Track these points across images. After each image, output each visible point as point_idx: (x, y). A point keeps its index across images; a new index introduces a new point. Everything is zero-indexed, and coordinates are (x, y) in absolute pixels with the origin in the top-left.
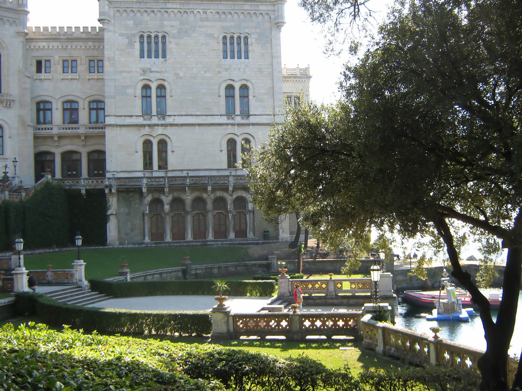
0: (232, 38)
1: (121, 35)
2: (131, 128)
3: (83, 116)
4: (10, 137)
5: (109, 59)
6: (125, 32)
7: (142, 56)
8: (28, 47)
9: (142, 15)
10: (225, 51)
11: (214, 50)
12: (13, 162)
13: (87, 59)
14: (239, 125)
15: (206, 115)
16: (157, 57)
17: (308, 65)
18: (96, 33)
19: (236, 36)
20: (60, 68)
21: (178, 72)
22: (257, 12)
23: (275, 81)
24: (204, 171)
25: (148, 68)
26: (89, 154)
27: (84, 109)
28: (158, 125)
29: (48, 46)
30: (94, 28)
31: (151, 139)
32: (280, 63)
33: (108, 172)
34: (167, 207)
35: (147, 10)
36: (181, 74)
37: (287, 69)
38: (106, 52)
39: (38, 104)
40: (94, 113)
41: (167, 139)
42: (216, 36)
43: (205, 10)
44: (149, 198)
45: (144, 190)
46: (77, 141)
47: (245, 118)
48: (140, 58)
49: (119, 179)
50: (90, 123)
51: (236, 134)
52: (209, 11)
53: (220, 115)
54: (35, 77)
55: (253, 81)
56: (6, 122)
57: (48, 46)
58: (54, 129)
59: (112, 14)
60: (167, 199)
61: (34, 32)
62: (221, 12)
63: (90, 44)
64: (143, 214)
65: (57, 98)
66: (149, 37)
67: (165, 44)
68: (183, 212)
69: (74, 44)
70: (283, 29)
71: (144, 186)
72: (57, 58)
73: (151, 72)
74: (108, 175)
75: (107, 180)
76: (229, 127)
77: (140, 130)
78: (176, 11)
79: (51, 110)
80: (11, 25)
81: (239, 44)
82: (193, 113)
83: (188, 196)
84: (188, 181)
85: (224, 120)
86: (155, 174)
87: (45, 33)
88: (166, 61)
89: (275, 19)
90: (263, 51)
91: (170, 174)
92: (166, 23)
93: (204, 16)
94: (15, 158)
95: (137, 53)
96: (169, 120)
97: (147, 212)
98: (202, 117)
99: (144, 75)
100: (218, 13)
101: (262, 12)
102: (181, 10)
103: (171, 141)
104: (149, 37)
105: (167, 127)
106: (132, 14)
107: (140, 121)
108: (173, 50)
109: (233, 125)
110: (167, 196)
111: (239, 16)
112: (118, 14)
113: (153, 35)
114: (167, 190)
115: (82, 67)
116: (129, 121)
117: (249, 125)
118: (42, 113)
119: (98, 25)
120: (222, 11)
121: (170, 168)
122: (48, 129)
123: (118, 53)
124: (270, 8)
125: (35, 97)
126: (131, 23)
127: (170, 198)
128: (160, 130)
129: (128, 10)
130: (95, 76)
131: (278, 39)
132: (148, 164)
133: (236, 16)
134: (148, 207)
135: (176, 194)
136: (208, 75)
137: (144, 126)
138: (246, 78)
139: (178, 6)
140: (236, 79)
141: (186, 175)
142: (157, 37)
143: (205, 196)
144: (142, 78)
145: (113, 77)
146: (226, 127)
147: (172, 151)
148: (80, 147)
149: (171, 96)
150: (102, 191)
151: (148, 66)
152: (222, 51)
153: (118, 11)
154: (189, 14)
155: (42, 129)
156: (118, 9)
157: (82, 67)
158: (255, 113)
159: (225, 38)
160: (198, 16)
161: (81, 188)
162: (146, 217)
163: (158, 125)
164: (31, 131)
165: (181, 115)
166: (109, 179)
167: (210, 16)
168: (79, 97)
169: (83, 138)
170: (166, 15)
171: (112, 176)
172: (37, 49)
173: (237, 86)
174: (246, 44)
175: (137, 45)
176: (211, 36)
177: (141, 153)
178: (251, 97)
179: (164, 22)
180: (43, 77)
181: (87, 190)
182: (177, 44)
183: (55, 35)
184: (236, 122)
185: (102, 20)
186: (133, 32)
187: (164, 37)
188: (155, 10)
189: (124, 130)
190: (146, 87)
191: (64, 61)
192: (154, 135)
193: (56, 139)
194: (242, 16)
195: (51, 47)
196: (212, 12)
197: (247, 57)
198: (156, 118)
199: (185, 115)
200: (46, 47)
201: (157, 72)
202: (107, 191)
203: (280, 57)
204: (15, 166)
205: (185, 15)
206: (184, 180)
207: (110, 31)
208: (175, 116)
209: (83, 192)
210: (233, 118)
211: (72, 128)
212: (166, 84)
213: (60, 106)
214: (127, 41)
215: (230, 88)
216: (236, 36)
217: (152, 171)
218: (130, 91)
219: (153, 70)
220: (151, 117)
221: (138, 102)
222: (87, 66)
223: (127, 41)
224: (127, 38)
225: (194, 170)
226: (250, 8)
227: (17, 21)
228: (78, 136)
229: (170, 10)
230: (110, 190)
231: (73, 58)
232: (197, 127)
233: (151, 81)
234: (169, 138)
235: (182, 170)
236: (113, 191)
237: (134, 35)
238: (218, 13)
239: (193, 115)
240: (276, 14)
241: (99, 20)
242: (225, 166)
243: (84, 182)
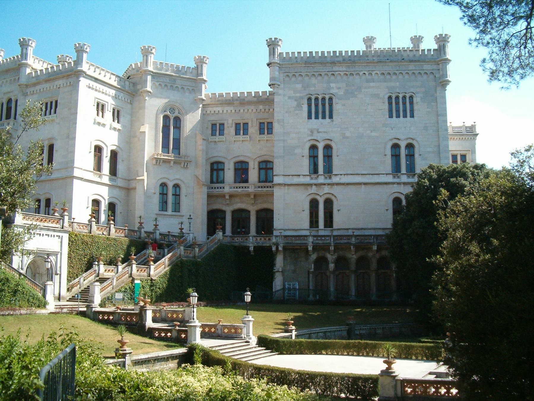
0: (397, 98)
1: (290, 98)
2: (298, 187)
3: (253, 175)
4: (186, 196)
5: (279, 121)
6: (294, 95)
7: (310, 117)
8: (205, 112)
9: (310, 78)
10: (390, 111)
11: (379, 110)
12: (188, 218)
13: (258, 122)
15: (372, 174)
16: (324, 117)
17: (475, 123)
18: (266, 97)
19: (401, 96)
20: (233, 130)
21: (344, 132)
22: (422, 72)
23: (441, 139)
24: (369, 230)
26: (258, 212)
27: (254, 169)
28: (325, 184)
29: (223, 111)
30: (264, 93)
31: (318, 198)
32: (446, 121)
33: (275, 230)
34: (332, 266)
36: (348, 134)
37: (453, 128)
38: (275, 115)
39: (212, 164)
40: (263, 172)
41: (333, 198)
42: (381, 96)
43: (370, 72)
44: (314, 257)
45: (310, 248)
47: (411, 177)
48: (308, 119)
49: (286, 237)
50: (259, 182)
51: (402, 193)
52: (375, 72)
53: (387, 174)
54: (210, 140)
55: (418, 139)
56: (183, 182)
57: (223, 111)
58: (225, 188)
59: (282, 78)
60: (331, 257)
61: (211, 98)
62: (386, 73)
63: (261, 107)
64: (309, 273)
65: (230, 158)
66: (317, 99)
67: (332, 105)
68: (348, 271)
69: (246, 108)
70: (448, 88)
71: (310, 244)
72: (230, 121)
73: (319, 132)
74: (275, 233)
75: (274, 237)
76: (395, 186)
77: (307, 189)
78: (342, 73)
79: (223, 170)
80: (190, 93)
81: (404, 103)
83: (353, 255)
84: (353, 239)
85: (390, 179)
86: (321, 233)
87: (220, 98)
89: (440, 78)
90: (428, 110)
91: (335, 233)
92: (332, 85)
93: (370, 77)
94: (190, 216)
95: (305, 114)
96: (335, 180)
97: (312, 270)
98: (368, 176)
99: (312, 135)
100: (383, 74)
101: (426, 72)
102: (347, 73)
103: (337, 200)
104: (317, 99)
105: (333, 186)
106: (300, 78)
107: (307, 180)
109: (399, 184)
110: (332, 255)
111: (404, 77)
112: (287, 79)
113: (320, 97)
114: (333, 249)
115: (253, 129)
116: (296, 180)
118: (215, 173)
119: (269, 89)
120: (387, 72)
121: (335, 226)
122: (221, 188)
123: (287, 115)
124: (435, 67)
125: (210, 158)
126: (299, 86)
127: (335, 257)
128: (326, 189)
129: (297, 74)
130: (265, 137)
131: (444, 97)
132: (314, 222)
133: (401, 77)
134: (313, 265)
135: (341, 253)
136: (374, 134)
137: (311, 185)
138: (411, 137)
139: (344, 69)
141: (352, 234)
142: (324, 99)
143: (370, 254)
145: (282, 138)
147: (339, 210)
149: (337, 156)
150: (270, 247)
151: (315, 127)
152: (387, 110)
153: (288, 76)
154: (355, 76)
155: (215, 188)
157: (253, 129)
159: (390, 98)
160: (364, 77)
161: (250, 245)
162: (311, 275)
163: (325, 184)
164: (205, 190)
165: (347, 174)
166: (276, 236)
167: (376, 77)
169: (252, 197)
170: (332, 78)
171: (279, 234)
172: (212, 114)
173: (403, 145)
174: (411, 103)
175: (305, 107)
176: (376, 96)
177: (307, 213)
178: (416, 156)
179: (331, 84)
180: (217, 140)
181: (255, 247)
182: (344, 105)
183: (230, 100)
185: (273, 85)
186: (301, 95)
187: (331, 99)
188: (323, 74)
189: (292, 188)
190: (314, 148)
191: (236, 124)
192: (321, 194)
193: (227, 197)
194: (407, 77)
195: (225, 112)
196: (376, 73)
197: (412, 116)
198: (323, 177)
199: (351, 174)
200: (221, 112)
201: (324, 132)
202: (274, 249)
203: (445, 115)
204: (190, 223)
205: (351, 77)
206: (349, 239)
207: (280, 95)
208: (341, 175)
209: (252, 249)
210: (398, 177)
211: (242, 188)
214: (296, 103)
215: (396, 147)
216: (401, 96)
217: (318, 230)
219: (320, 130)
220: (318, 177)
221: (306, 162)
222: (257, 128)
223: (296, 103)
224: (296, 100)
225: (359, 229)
226: (414, 68)
227: (195, 88)
228: (248, 195)
229: (337, 73)
230: (277, 248)
231: (244, 121)
232: (363, 186)
234: (335, 197)
235: (347, 229)
236: (280, 248)
237: (302, 98)
238: (383, 74)
240: (441, 72)
241: (270, 85)
243: (253, 240)
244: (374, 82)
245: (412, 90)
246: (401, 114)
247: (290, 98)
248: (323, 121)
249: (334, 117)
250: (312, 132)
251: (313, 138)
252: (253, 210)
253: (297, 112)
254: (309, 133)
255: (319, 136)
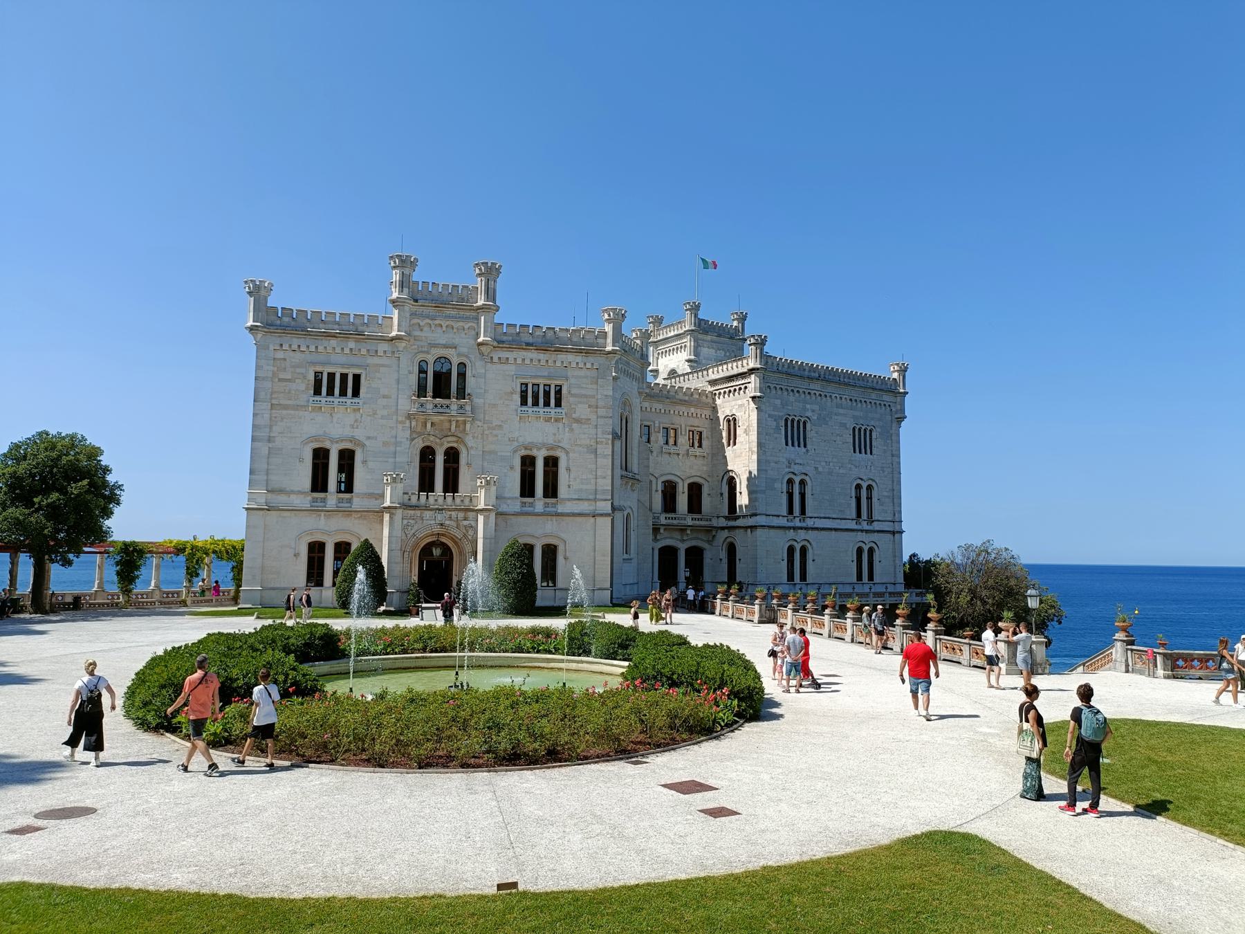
1: (770, 416)
7: (787, 444)
14: (867, 531)
25: (793, 460)
26: (687, 551)
29: (651, 408)
31: (795, 543)
35: (777, 386)
36: (820, 469)
41: (808, 545)
46: (677, 535)
57: (651, 408)
73: (795, 464)
76: (859, 533)
82: (830, 516)
88: (807, 451)
92: (808, 406)
96: (810, 523)
99: (790, 467)
100: (851, 400)
102: (822, 393)
107: (783, 522)
108: (814, 439)
117: (874, 531)
126: (778, 402)
128: (802, 534)
131: (898, 435)
137: (789, 528)
140: (864, 478)
144: (787, 470)
146: (855, 533)
147: (813, 560)
148: (678, 542)
151: (793, 456)
156: (769, 384)
157: (683, 440)
158: (880, 519)
159: (854, 429)
163: (801, 528)
165: (821, 518)
168: (679, 477)
173: (865, 485)
175: (783, 429)
178: (875, 500)
184: (864, 528)
186: (781, 414)
188: (801, 391)
189: (772, 531)
192: (799, 541)
195: (653, 410)
199: (825, 518)
205: (824, 399)
212: (807, 479)
213: (660, 488)
215: (858, 487)
216: (863, 428)
218: (778, 485)
221: (784, 498)
224: (775, 420)
228: (682, 530)
233: (795, 474)
239: (829, 518)
242: (855, 580)
244: (842, 408)
245: (872, 423)
246: (863, 450)
247: (770, 416)
248: (793, 448)
249: (809, 446)
250: (790, 463)
251: (792, 470)
252: (682, 548)
253: (775, 435)
254: (786, 463)
255: (796, 469)
